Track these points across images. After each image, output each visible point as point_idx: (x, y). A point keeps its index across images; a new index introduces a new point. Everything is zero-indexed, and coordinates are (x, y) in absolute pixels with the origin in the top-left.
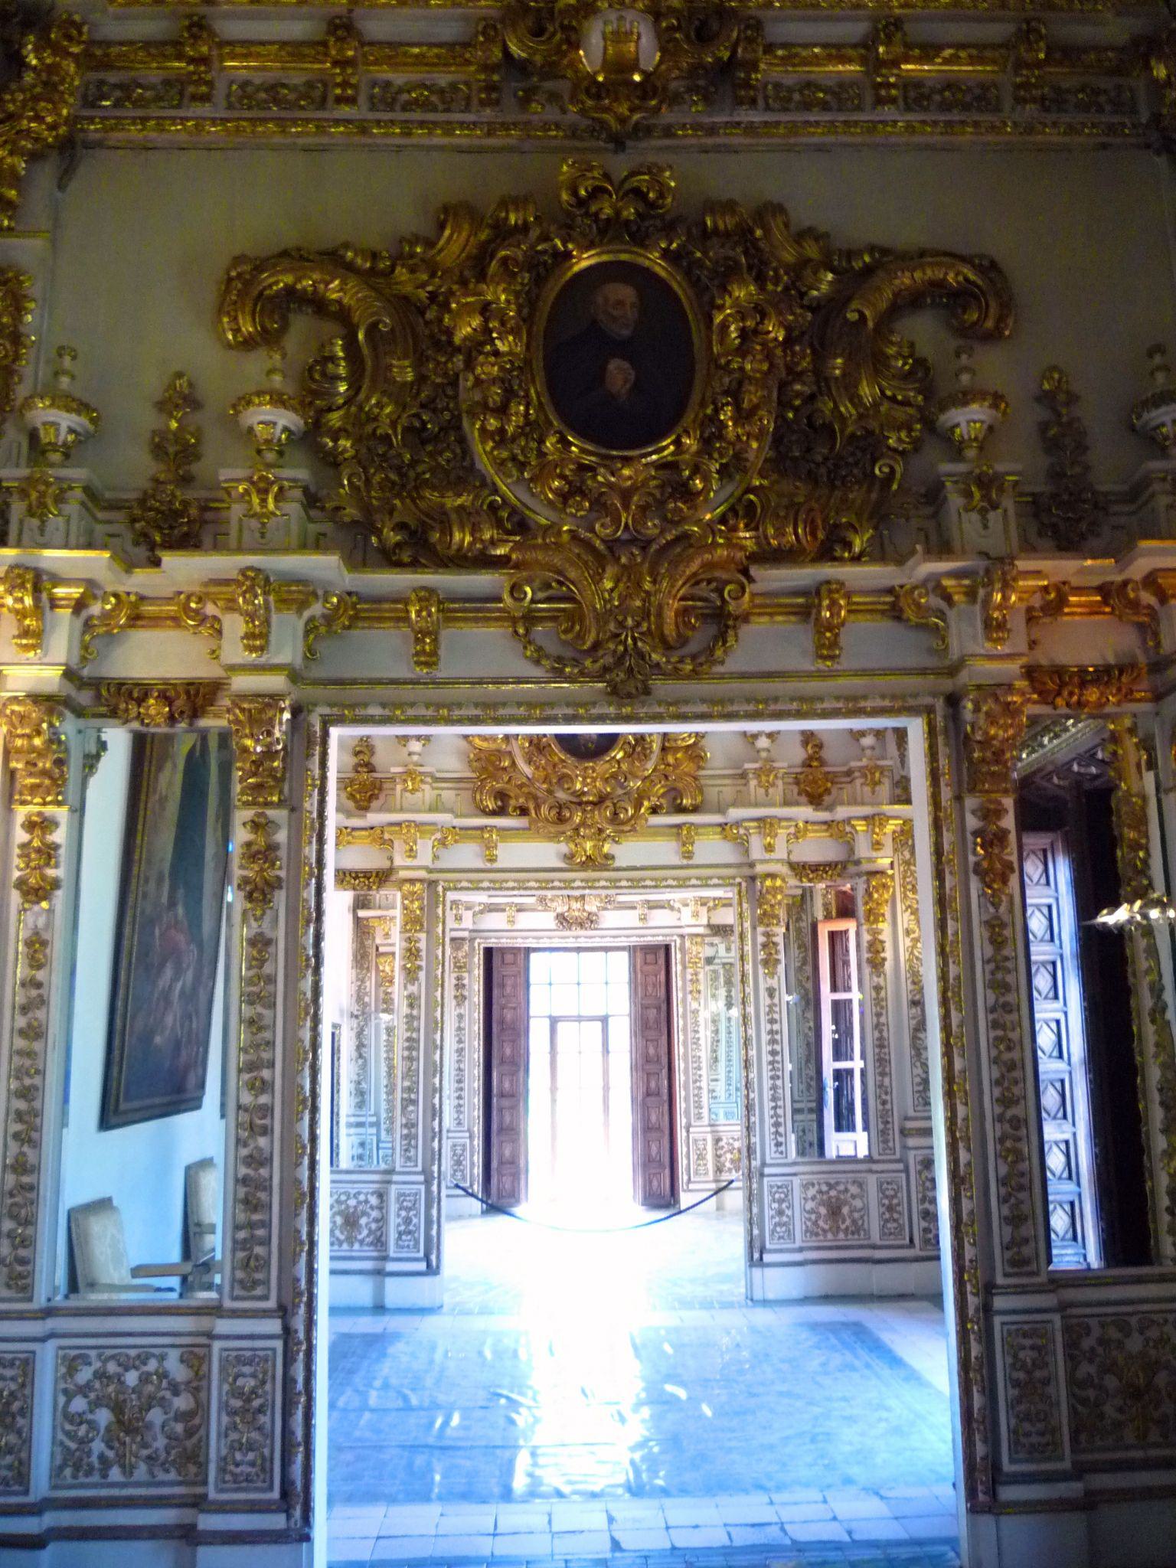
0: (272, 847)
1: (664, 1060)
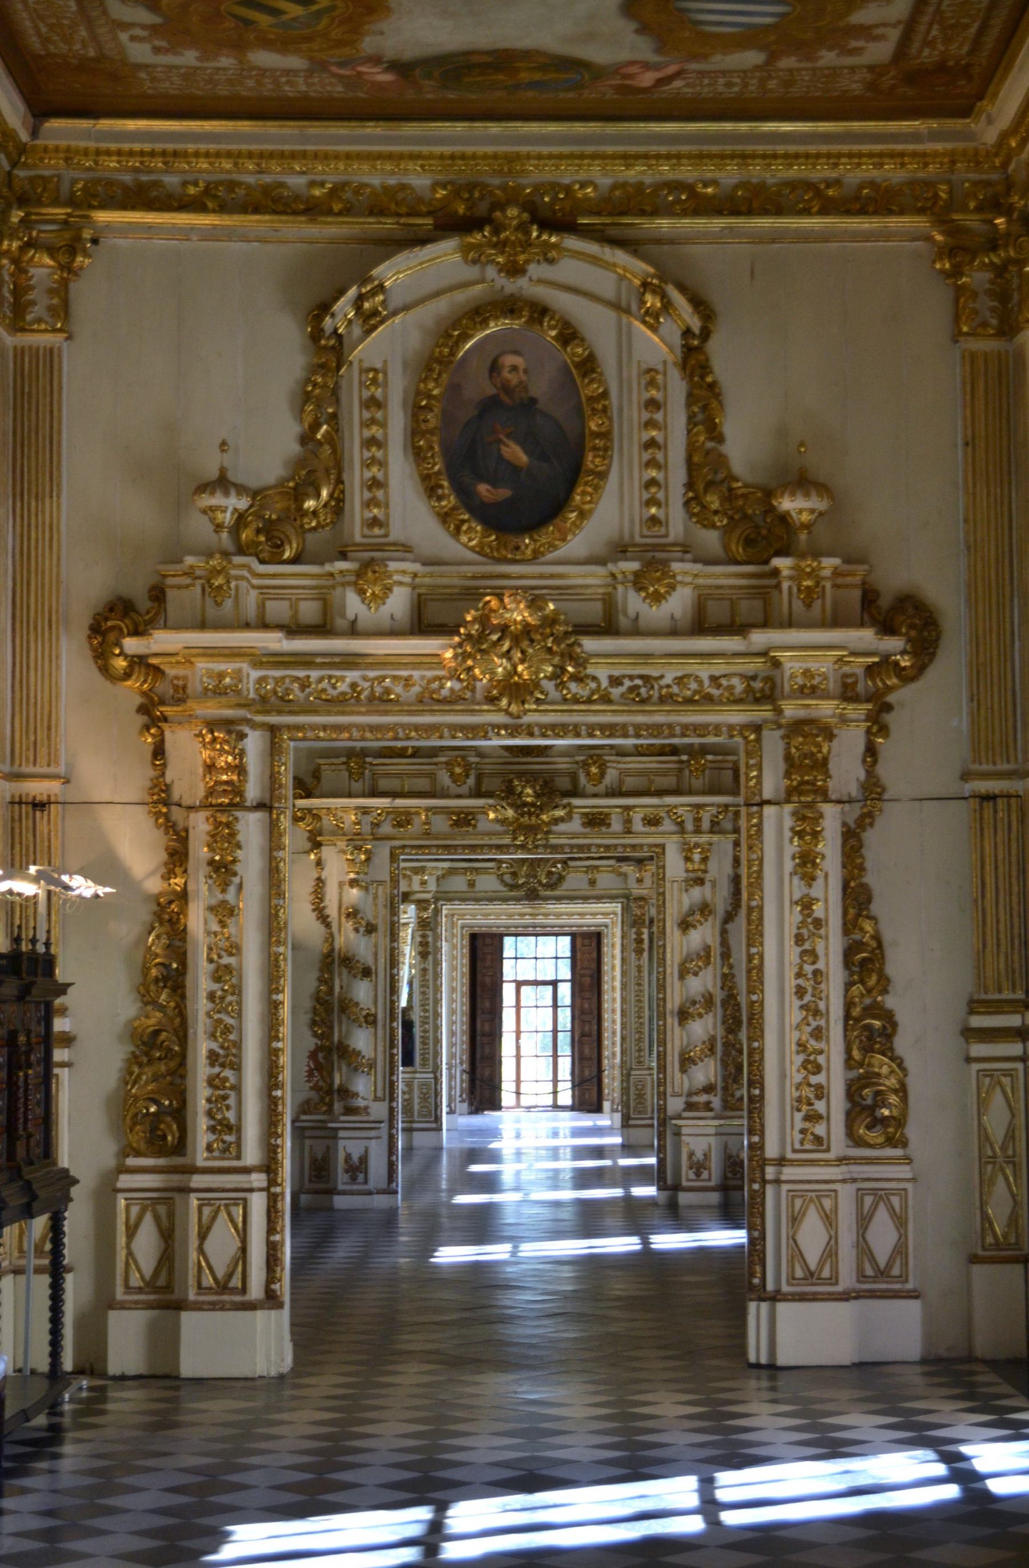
0: (427, 943)
1: (596, 1012)
